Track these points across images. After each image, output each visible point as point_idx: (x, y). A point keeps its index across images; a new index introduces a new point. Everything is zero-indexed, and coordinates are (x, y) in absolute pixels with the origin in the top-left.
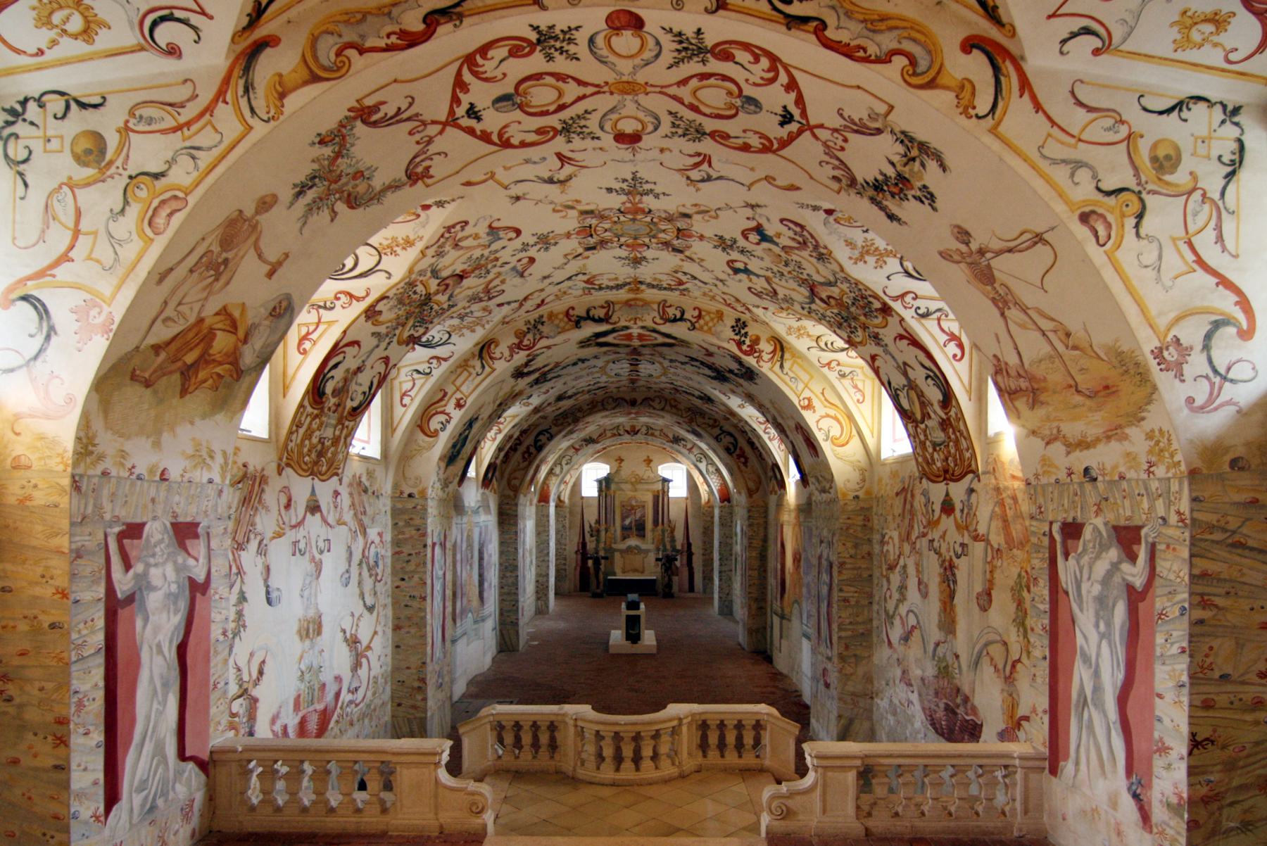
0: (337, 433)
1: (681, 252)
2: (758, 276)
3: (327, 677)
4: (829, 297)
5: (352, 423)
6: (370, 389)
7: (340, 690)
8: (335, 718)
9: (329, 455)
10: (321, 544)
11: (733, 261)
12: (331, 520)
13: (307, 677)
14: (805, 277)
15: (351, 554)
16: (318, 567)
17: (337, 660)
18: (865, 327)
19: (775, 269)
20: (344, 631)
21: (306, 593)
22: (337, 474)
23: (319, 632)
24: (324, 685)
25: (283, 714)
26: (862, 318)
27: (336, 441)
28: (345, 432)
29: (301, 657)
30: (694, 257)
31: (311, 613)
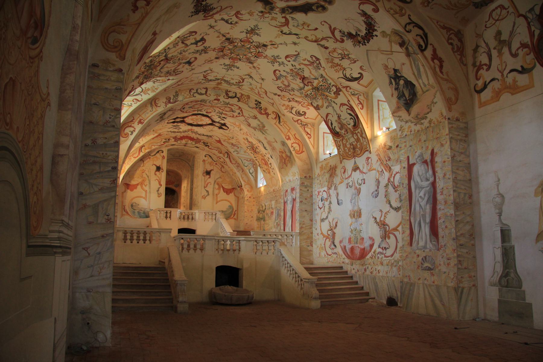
0: (356, 137)
1: (228, 39)
2: (192, 44)
3: (364, 235)
4: (160, 64)
5: (359, 130)
6: (351, 115)
7: (373, 244)
8: (370, 255)
9: (359, 146)
10: (360, 182)
11: (203, 43)
12: (364, 171)
13: (354, 232)
14: (171, 62)
15: (379, 182)
16: (359, 191)
17: (372, 231)
18: (143, 73)
19: (184, 53)
20: (375, 219)
21: (353, 201)
22: (367, 151)
23: (360, 215)
24: (363, 239)
25: (344, 241)
26: (146, 73)
27: (358, 140)
28: (359, 135)
29: (351, 224)
30: (221, 37)
31: (356, 208)
